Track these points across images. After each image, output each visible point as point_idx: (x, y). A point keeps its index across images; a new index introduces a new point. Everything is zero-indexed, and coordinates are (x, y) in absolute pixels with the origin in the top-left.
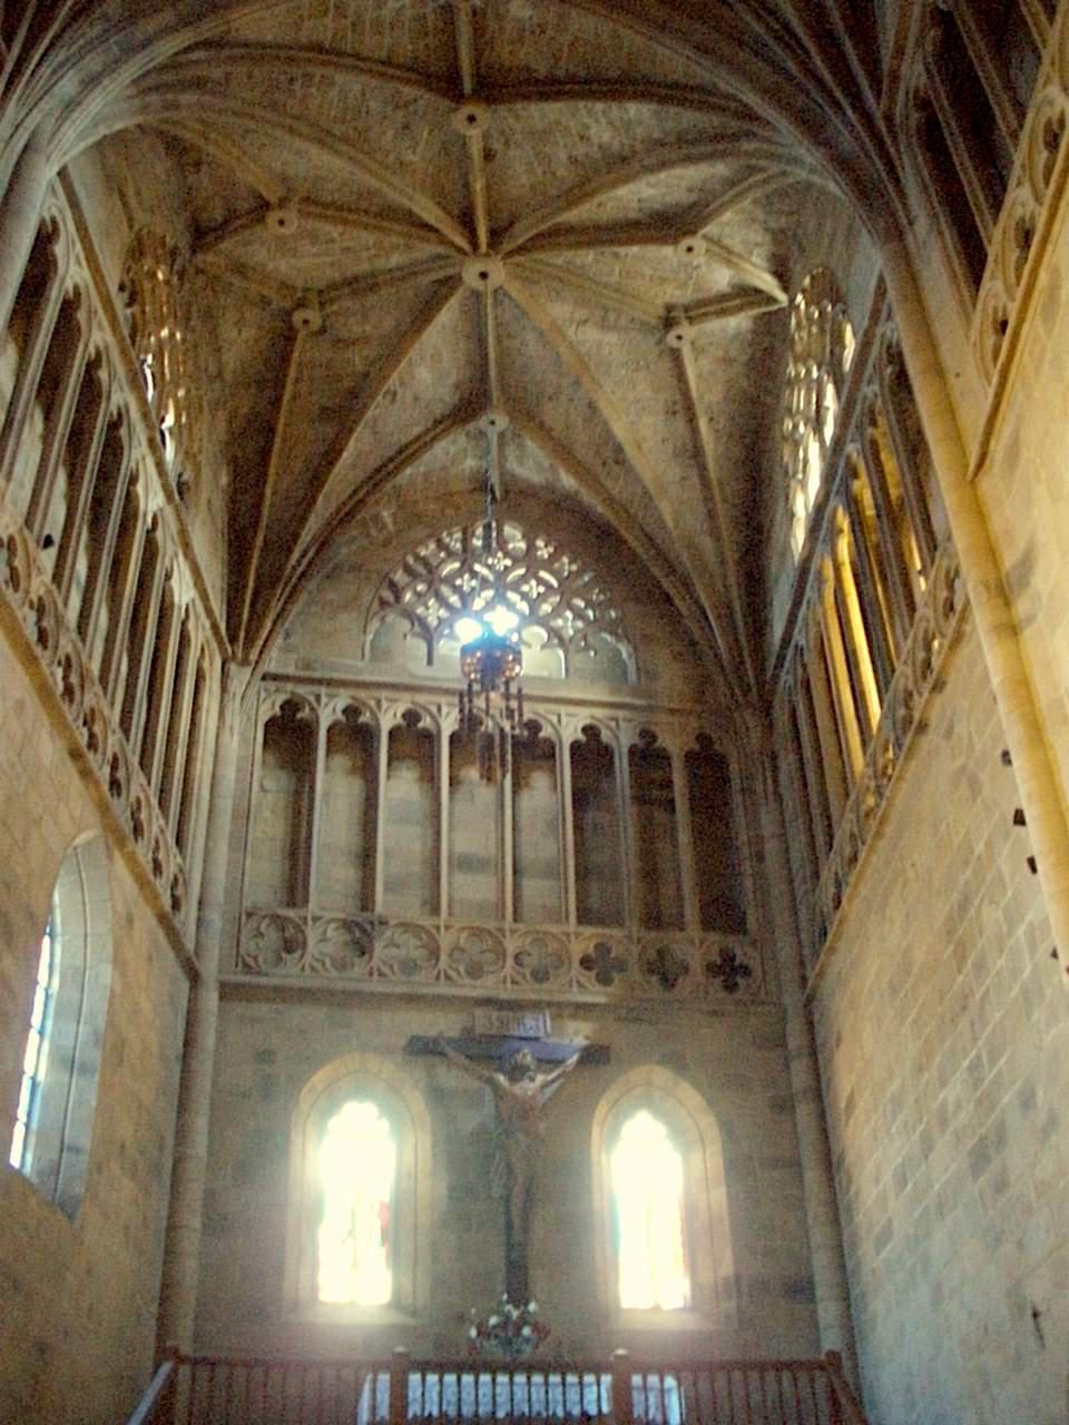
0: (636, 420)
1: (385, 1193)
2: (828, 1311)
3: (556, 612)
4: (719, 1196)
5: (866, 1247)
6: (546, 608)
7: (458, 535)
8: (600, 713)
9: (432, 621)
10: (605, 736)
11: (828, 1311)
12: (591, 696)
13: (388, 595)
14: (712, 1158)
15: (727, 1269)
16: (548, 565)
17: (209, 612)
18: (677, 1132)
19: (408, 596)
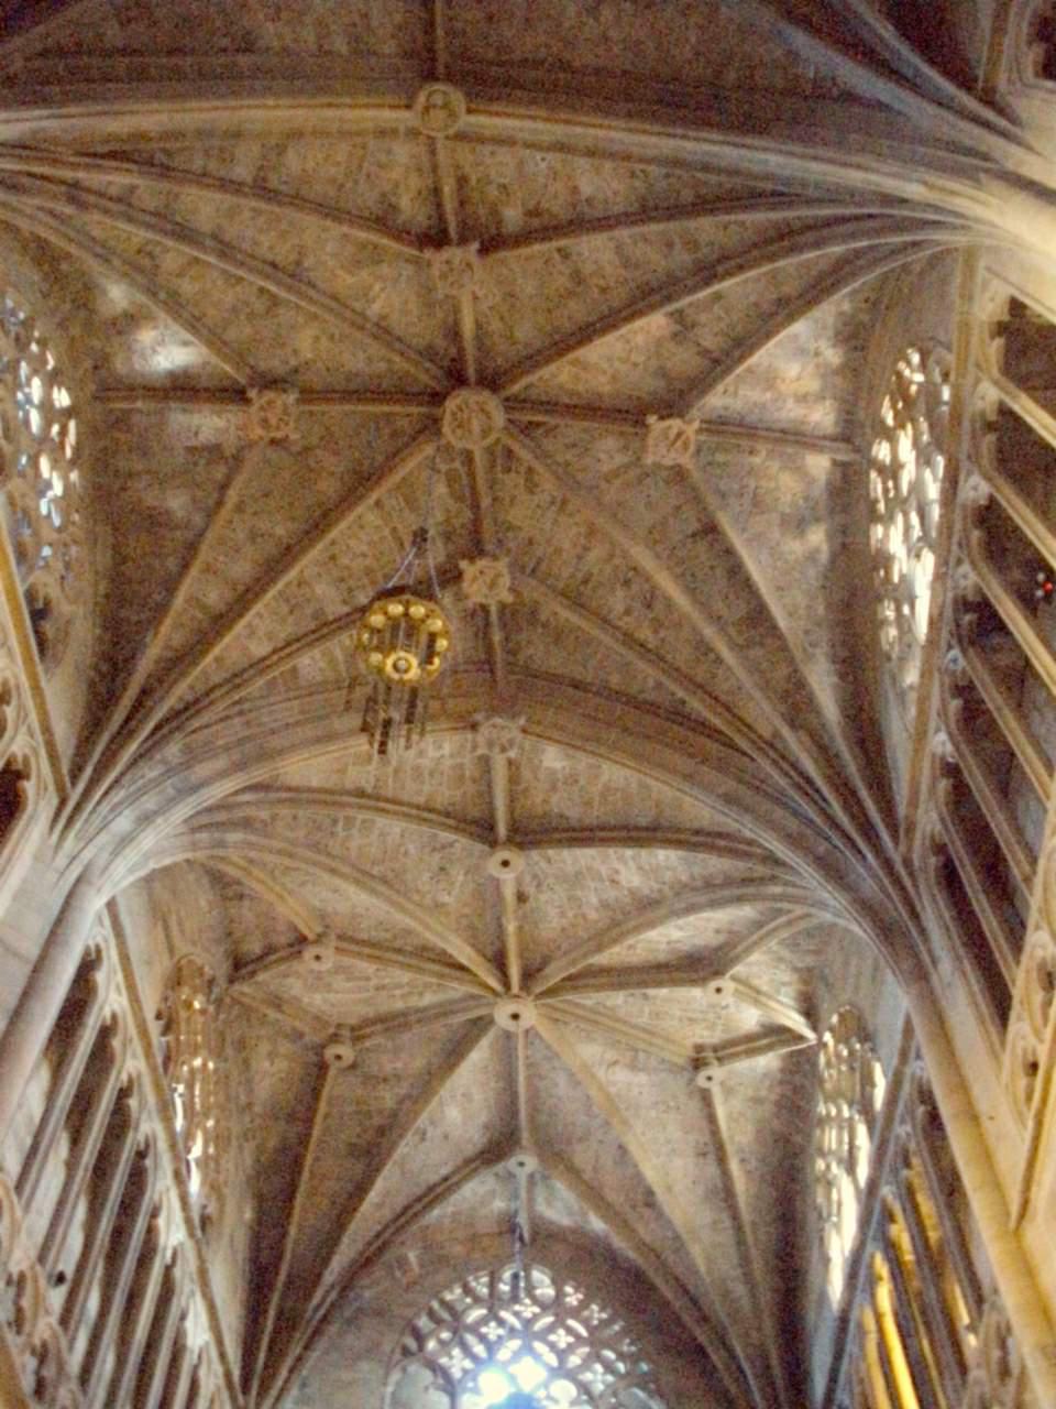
0: (667, 1164)
3: (586, 1365)
6: (574, 1360)
7: (485, 1280)
9: (456, 1373)
13: (412, 1344)
16: (575, 1313)
17: (222, 1356)
19: (431, 1345)
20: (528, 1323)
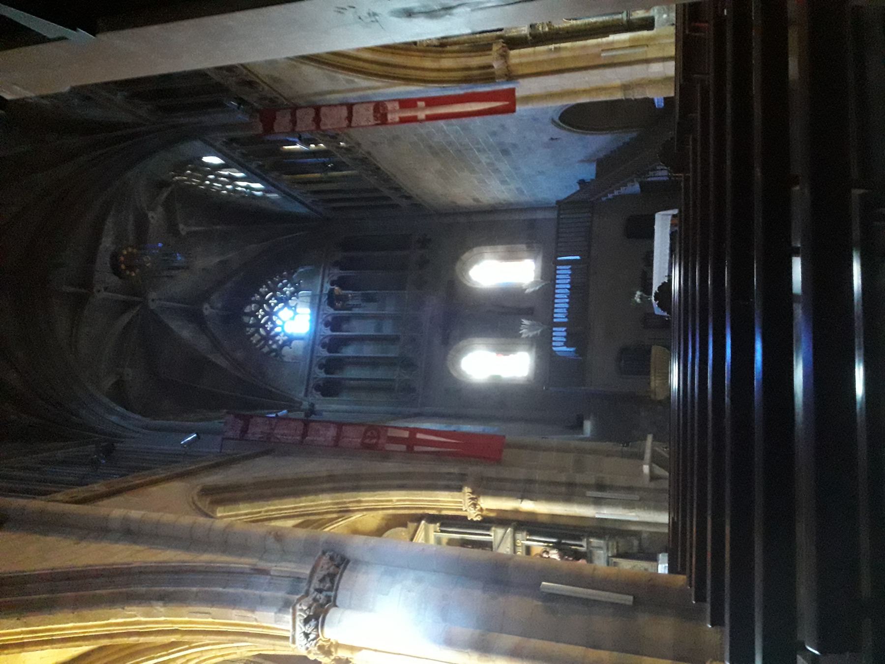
0: (207, 260)
1: (494, 354)
2: (539, 215)
4: (501, 248)
5: (523, 199)
7: (248, 329)
8: (326, 280)
9: (286, 338)
10: (335, 278)
11: (539, 215)
12: (320, 282)
14: (487, 250)
15: (524, 246)
18: (476, 262)
19: (274, 346)
20: (266, 313)
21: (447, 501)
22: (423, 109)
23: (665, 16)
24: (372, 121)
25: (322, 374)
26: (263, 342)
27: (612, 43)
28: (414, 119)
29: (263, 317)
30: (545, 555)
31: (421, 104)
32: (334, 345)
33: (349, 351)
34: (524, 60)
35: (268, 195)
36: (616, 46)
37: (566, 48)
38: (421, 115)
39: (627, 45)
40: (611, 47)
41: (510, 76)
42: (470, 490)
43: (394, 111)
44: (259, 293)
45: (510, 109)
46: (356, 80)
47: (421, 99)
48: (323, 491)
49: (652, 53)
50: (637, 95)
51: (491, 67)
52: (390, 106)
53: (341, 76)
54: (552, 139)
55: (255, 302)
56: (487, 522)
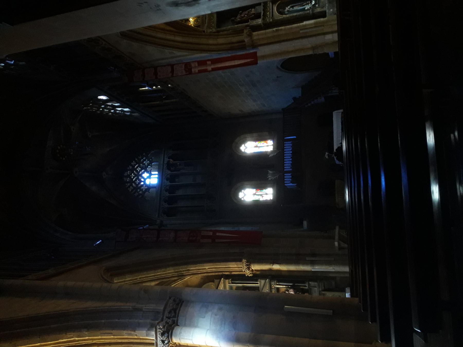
4: (255, 135)
8: (166, 156)
9: (146, 187)
13: (140, 196)
15: (267, 133)
19: (141, 192)
20: (136, 175)
21: (235, 267)
22: (210, 65)
23: (331, 10)
24: (184, 73)
25: (166, 205)
26: (134, 191)
27: (306, 25)
28: (206, 71)
29: (134, 177)
30: (287, 292)
31: (209, 63)
32: (171, 190)
33: (180, 192)
34: (260, 37)
35: (133, 114)
36: (308, 27)
37: (281, 29)
38: (209, 68)
39: (313, 26)
40: (305, 27)
41: (254, 46)
42: (245, 261)
43: (195, 67)
44: (132, 165)
45: (255, 63)
46: (174, 52)
47: (209, 60)
48: (169, 266)
49: (326, 30)
50: (320, 52)
51: (244, 41)
52: (193, 65)
53: (166, 51)
54: (278, 77)
55: (130, 170)
56: (256, 276)
